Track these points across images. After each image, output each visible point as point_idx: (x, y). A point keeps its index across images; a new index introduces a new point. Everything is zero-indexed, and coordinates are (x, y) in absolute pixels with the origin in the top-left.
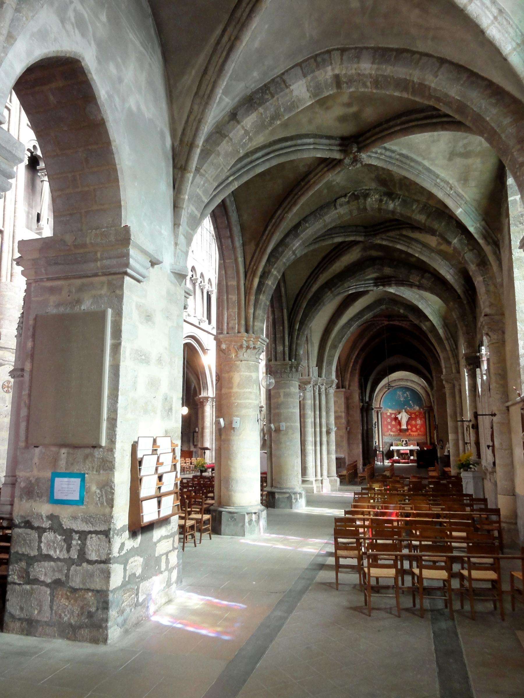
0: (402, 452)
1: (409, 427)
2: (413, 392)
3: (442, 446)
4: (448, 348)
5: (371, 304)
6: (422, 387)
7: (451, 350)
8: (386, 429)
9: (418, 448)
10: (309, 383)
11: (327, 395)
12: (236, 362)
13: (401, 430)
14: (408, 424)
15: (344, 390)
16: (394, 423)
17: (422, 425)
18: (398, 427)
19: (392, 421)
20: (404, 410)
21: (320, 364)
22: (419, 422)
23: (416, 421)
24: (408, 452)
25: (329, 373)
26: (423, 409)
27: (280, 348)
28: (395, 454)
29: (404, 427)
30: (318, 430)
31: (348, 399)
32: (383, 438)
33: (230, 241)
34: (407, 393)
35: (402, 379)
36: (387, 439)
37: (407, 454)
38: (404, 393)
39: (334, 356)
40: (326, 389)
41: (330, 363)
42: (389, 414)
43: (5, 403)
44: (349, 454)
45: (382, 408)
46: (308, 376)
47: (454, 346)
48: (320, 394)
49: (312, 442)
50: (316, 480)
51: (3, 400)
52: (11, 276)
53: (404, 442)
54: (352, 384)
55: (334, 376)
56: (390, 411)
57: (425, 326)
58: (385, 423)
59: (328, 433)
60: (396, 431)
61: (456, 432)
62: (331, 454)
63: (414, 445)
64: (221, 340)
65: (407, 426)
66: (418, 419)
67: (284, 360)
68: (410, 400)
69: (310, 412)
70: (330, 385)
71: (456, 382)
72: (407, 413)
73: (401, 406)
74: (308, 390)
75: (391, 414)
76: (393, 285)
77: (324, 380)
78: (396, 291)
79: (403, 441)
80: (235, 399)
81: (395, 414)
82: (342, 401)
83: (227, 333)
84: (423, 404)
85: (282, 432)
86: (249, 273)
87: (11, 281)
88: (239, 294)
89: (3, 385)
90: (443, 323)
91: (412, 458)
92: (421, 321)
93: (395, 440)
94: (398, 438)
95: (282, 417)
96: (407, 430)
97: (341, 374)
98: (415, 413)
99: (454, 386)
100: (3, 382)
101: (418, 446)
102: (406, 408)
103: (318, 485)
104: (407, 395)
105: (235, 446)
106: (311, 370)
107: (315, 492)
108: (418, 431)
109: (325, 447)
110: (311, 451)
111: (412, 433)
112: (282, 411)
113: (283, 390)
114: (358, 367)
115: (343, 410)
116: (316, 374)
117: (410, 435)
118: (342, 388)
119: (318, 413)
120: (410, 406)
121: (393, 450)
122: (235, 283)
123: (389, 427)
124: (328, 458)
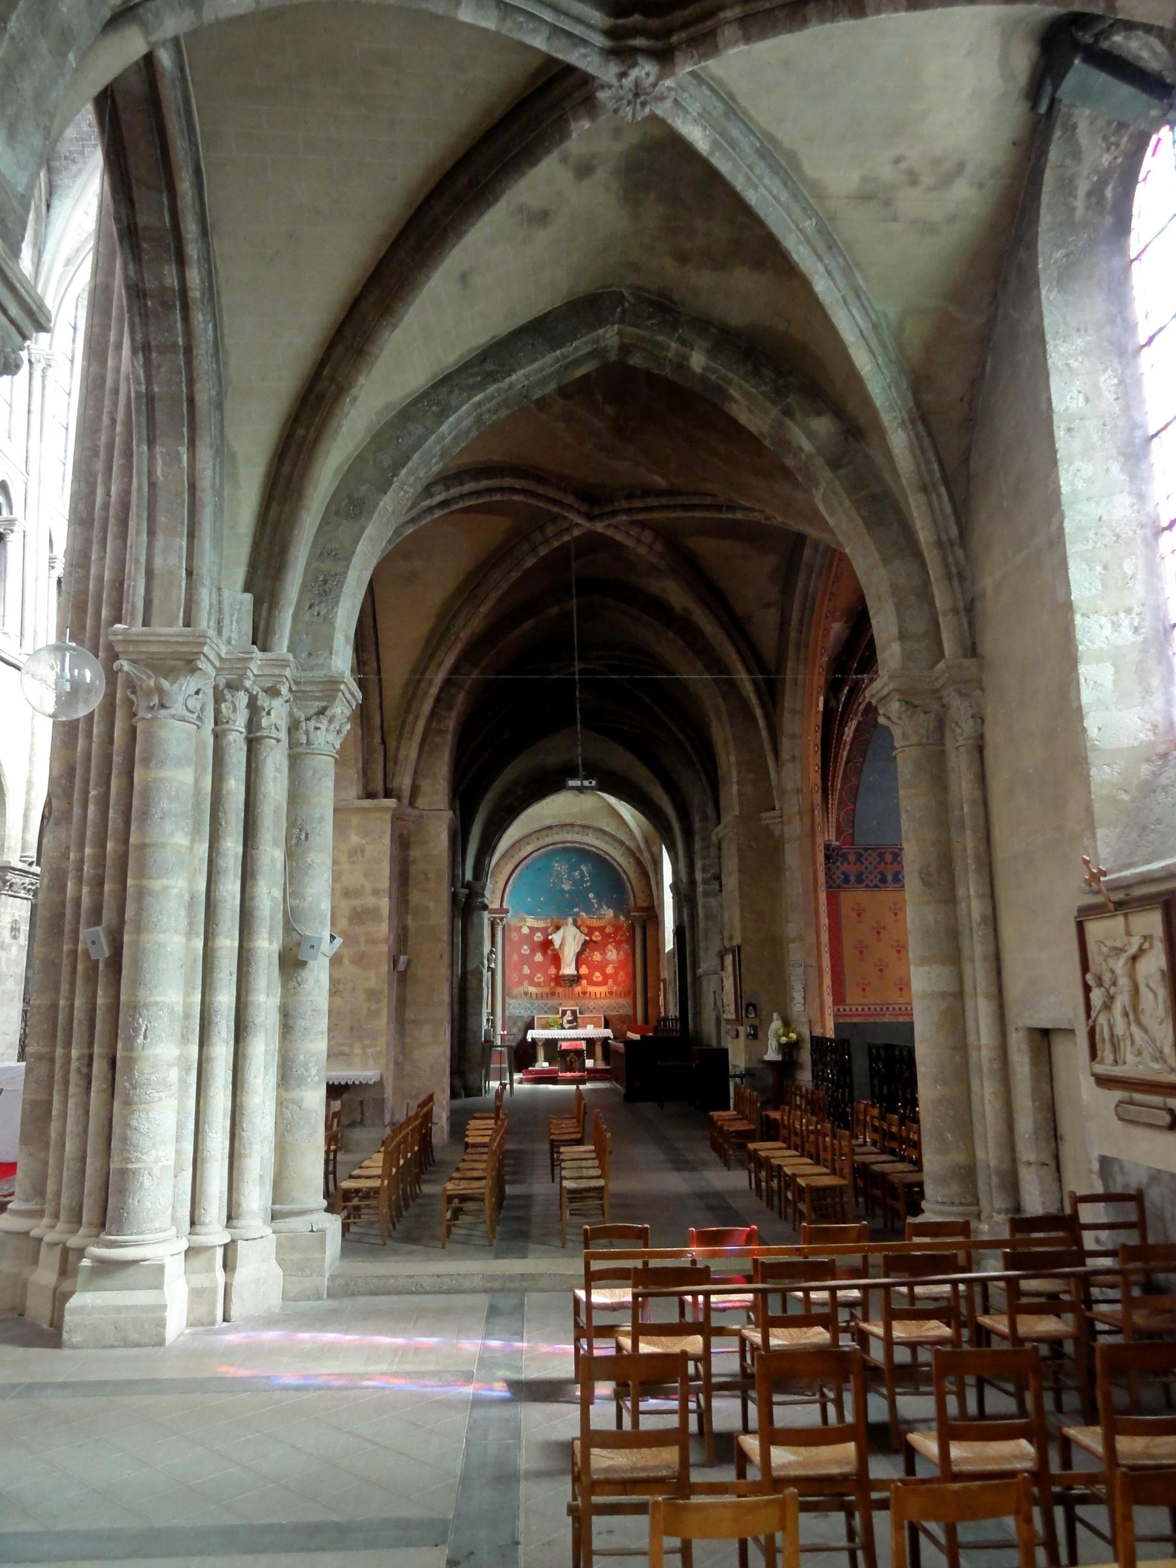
0: (564, 1046)
1: (584, 970)
2: (599, 861)
3: (755, 1028)
4: (924, 535)
5: (546, 316)
6: (628, 849)
7: (940, 544)
8: (515, 977)
10: (189, 665)
11: (295, 760)
13: (559, 980)
14: (579, 959)
15: (391, 803)
16: (539, 957)
17: (620, 965)
18: (552, 971)
19: (533, 952)
20: (570, 920)
21: (264, 576)
22: (612, 954)
23: (603, 953)
24: (583, 1045)
25: (312, 641)
26: (628, 916)
28: (541, 1054)
29: (569, 969)
30: (228, 943)
31: (403, 844)
32: (512, 1003)
34: (583, 868)
35: (572, 825)
36: (518, 1008)
37: (578, 1053)
38: (571, 870)
39: (344, 557)
40: (294, 726)
41: (323, 588)
42: (525, 931)
44: (399, 1066)
45: (507, 911)
46: (187, 624)
47: (954, 531)
48: (253, 744)
49: (187, 1016)
50: (191, 1252)
53: (568, 1017)
54: (425, 785)
55: (341, 659)
56: (531, 922)
57: (811, 435)
58: (515, 957)
59: (291, 963)
60: (546, 984)
61: (954, 958)
62: (301, 1081)
63: (596, 1026)
65: (577, 969)
66: (610, 947)
68: (589, 890)
69: (181, 839)
70: (317, 705)
71: (958, 706)
72: (578, 928)
73: (564, 906)
74: (178, 708)
75: (533, 930)
76: (728, 32)
77: (283, 663)
78: (715, 144)
79: (564, 1013)
81: (545, 931)
82: (381, 847)
84: (627, 901)
90: (911, 404)
91: (589, 1063)
92: (788, 413)
93: (541, 1010)
94: (551, 1002)
96: (576, 979)
97: (383, 742)
98: (601, 929)
99: (941, 726)
101: (606, 1027)
102: (578, 914)
103: (200, 1281)
104: (582, 874)
106: (205, 596)
107: (176, 1325)
108: (610, 982)
109: (262, 1049)
110: (174, 1074)
111: (591, 989)
114: (451, 723)
115: (385, 884)
116: (239, 627)
117: (584, 993)
118: (388, 794)
119: (232, 845)
120: (589, 908)
124: (281, 1104)
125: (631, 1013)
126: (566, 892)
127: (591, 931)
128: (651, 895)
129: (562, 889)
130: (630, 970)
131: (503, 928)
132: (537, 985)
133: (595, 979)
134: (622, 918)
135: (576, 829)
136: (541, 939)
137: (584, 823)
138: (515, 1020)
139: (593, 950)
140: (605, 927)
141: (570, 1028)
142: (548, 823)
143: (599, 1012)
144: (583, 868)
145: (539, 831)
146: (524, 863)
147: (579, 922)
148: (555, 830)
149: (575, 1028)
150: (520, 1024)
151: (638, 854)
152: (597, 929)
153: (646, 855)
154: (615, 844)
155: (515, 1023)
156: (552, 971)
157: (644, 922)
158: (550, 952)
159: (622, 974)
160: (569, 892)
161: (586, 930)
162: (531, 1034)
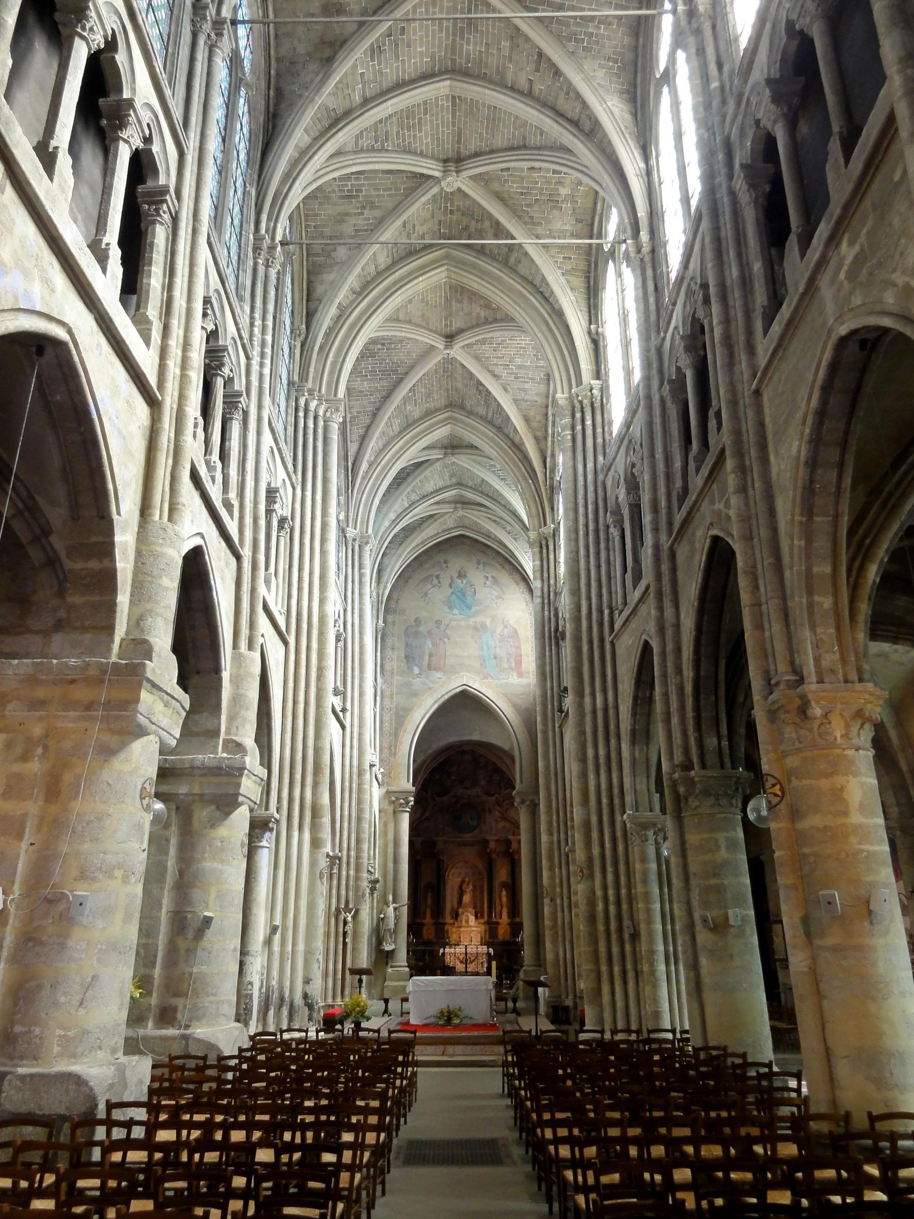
12: (847, 752)
27: (711, 742)
33: (834, 474)
43: (142, 842)
51: (139, 826)
52: (172, 510)
64: (810, 696)
67: (722, 766)
80: (860, 843)
83: (820, 681)
85: (732, 930)
86: (860, 553)
87: (170, 519)
88: (836, 594)
89: (143, 788)
95: (729, 896)
100: (143, 780)
105: (881, 964)
112: (726, 882)
113: (725, 834)
122: (828, 570)
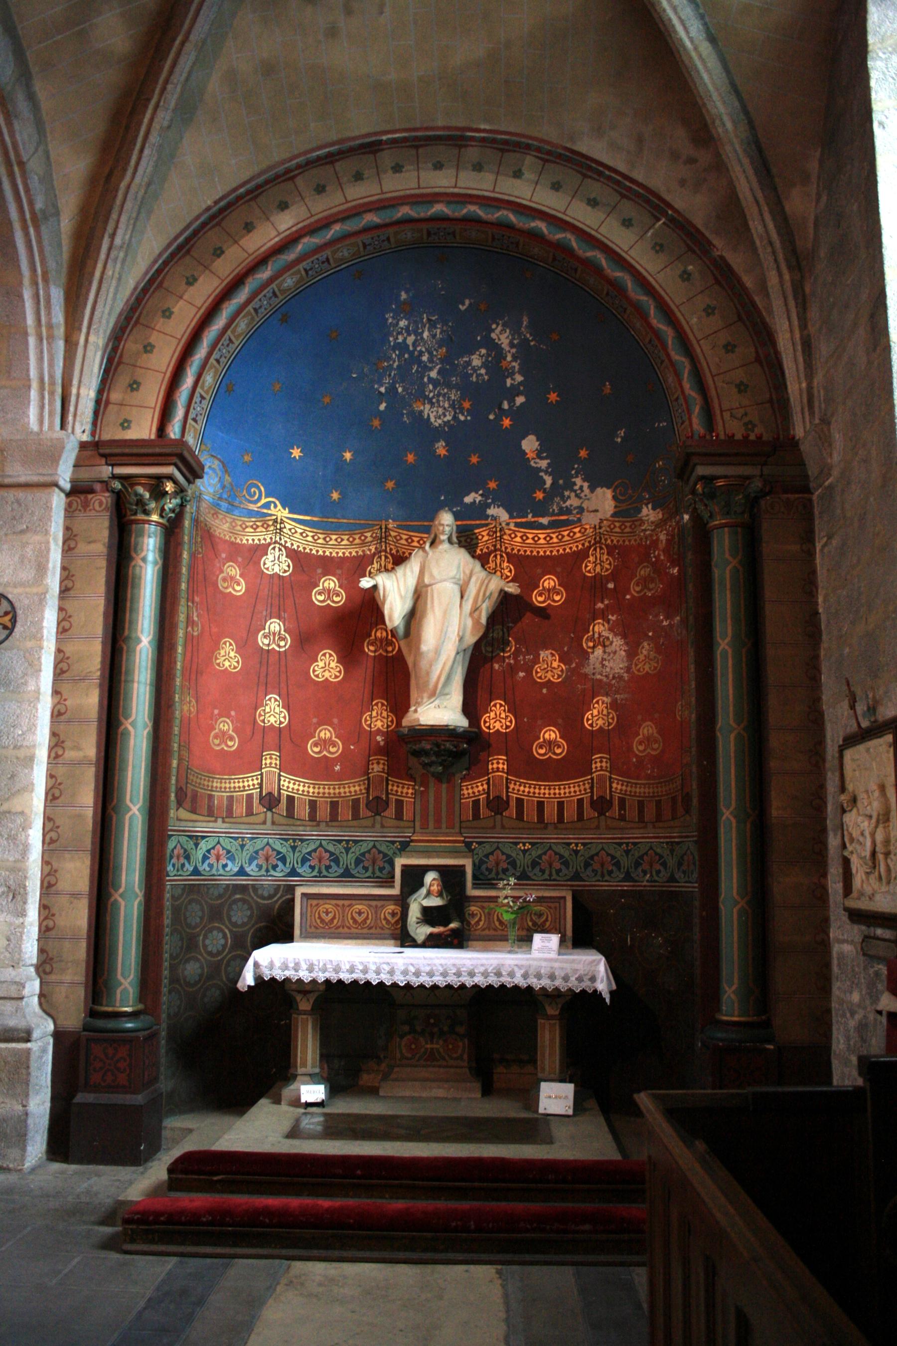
1: (498, 719)
6: (681, 226)
9: (592, 970)
14: (481, 670)
16: (326, 667)
17: (638, 698)
18: (377, 720)
19: (305, 643)
22: (609, 654)
23: (574, 654)
28: (308, 1047)
29: (440, 709)
34: (502, 337)
38: (458, 344)
42: (276, 564)
53: (430, 895)
56: (300, 535)
58: (229, 657)
60: (354, 767)
65: (470, 708)
66: (599, 628)
75: (307, 566)
79: (413, 879)
93: (331, 866)
94: (368, 837)
98: (567, 566)
101: (580, 938)
102: (479, 511)
108: (600, 763)
111: (523, 789)
117: (498, 804)
121: (274, 990)
123: (273, 712)
125: (689, 884)
126: (436, 433)
127: (527, 568)
128: (780, 404)
129: (421, 421)
130: (686, 711)
131: (171, 531)
132: (318, 770)
133: (539, 752)
134: (649, 514)
135: (472, 153)
136: (339, 600)
137: (508, 125)
138: (214, 901)
139: (533, 645)
140: (582, 555)
141: (433, 942)
142: (361, 124)
143: (550, 881)
144: (502, 337)
145: (330, 159)
146: (264, 274)
147: (484, 536)
148: (387, 158)
149: (456, 941)
150: (240, 915)
151: (720, 246)
152: (548, 564)
153: (761, 226)
154: (628, 208)
155: (216, 914)
156: (377, 720)
157: (753, 502)
158: (369, 650)
159: (648, 729)
160: (451, 432)
161: (508, 569)
162: (273, 960)
